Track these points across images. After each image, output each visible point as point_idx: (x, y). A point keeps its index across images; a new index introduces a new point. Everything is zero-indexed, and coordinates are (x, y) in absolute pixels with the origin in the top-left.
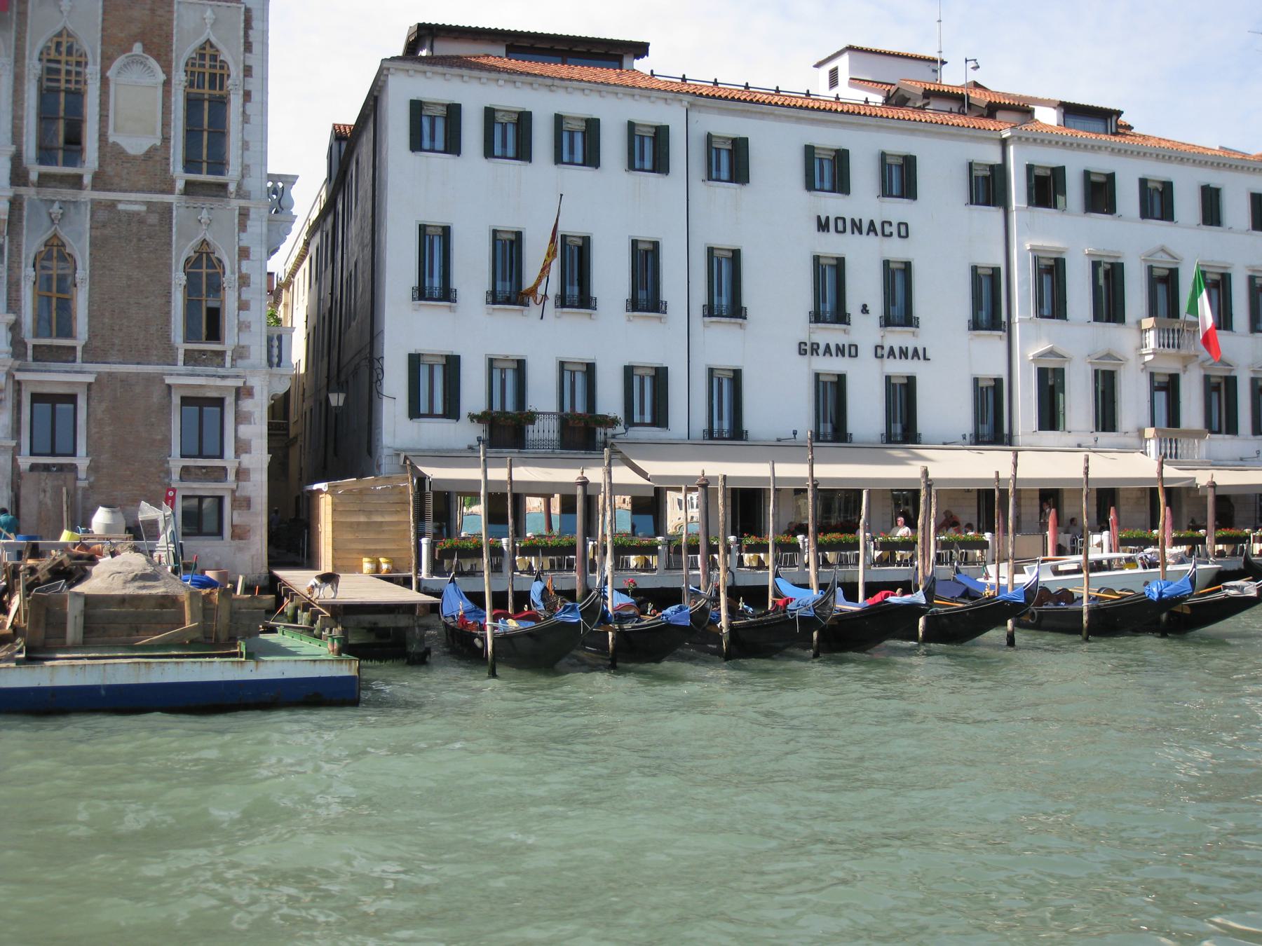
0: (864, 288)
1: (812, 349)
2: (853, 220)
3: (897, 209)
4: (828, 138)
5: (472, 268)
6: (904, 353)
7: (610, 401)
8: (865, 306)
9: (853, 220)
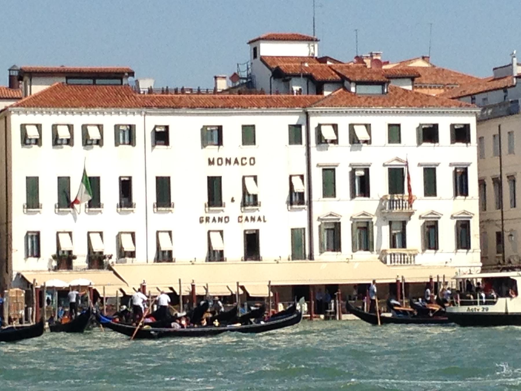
2: (227, 160)
3: (249, 151)
4: (213, 120)
5: (48, 194)
9: (227, 160)
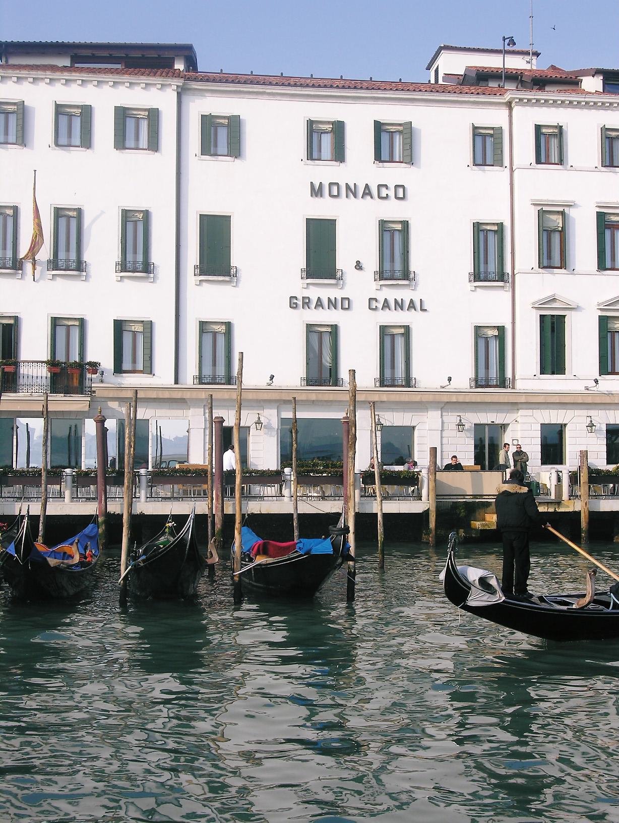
0: (356, 245)
1: (304, 303)
3: (393, 174)
6: (399, 305)
7: (100, 349)
8: (358, 262)
